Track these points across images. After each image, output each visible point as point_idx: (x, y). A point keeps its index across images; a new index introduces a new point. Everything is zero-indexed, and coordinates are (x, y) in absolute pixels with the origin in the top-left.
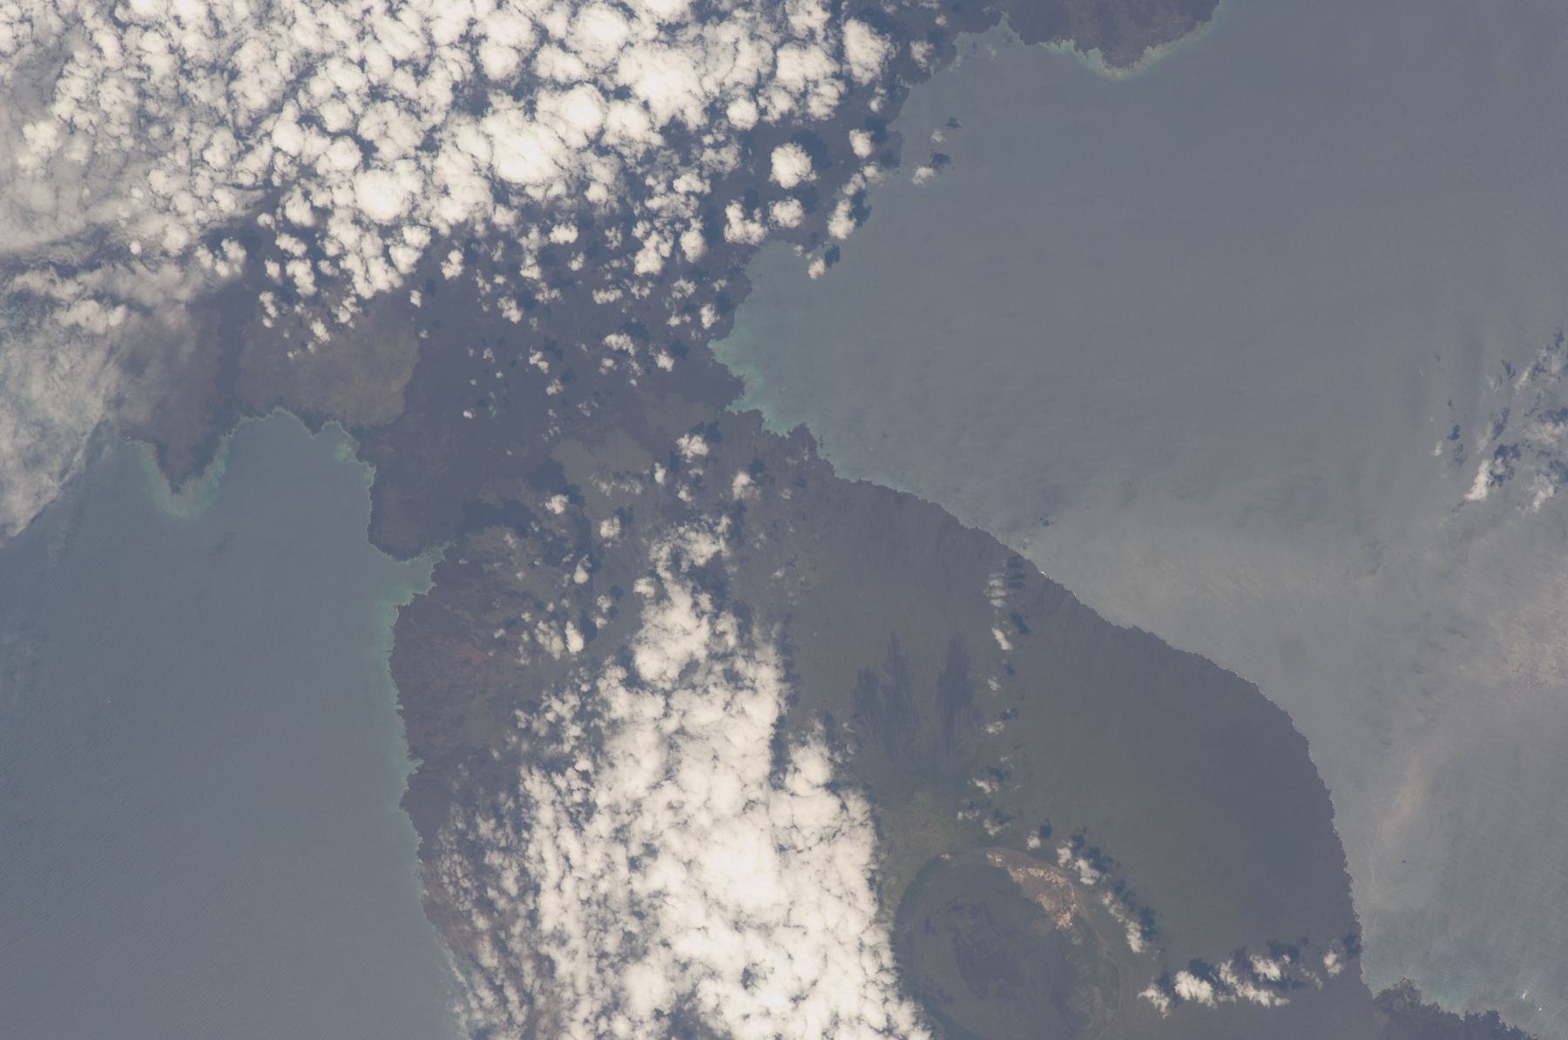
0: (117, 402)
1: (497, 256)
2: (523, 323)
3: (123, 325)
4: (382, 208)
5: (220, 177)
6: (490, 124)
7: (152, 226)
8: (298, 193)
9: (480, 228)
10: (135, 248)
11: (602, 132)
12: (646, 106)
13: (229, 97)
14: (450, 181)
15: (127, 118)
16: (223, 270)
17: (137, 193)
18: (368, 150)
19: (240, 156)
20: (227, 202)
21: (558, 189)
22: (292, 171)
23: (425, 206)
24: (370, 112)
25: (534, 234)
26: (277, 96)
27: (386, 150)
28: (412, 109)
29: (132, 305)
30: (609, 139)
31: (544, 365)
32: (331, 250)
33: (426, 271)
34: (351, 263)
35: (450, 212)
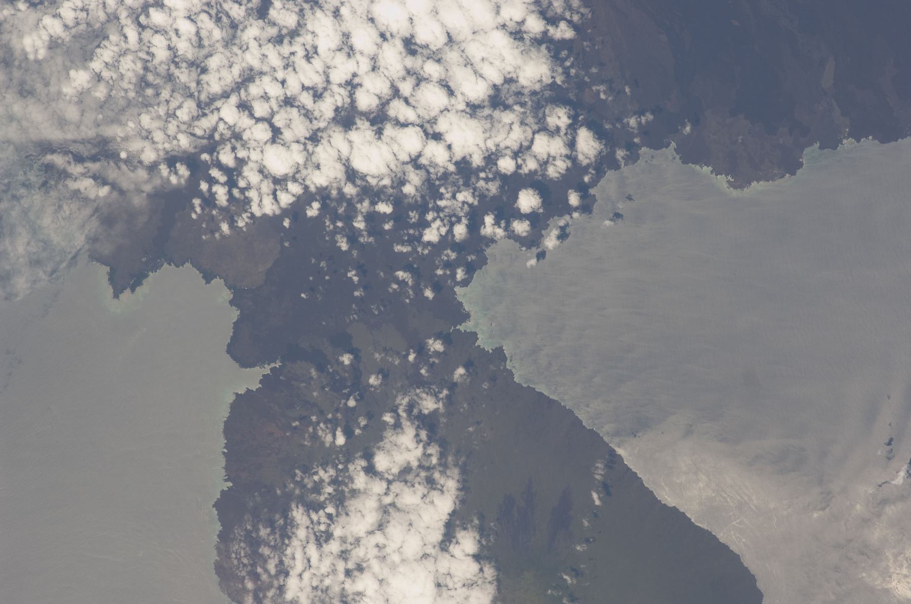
0: (93, 240)
1: (341, 210)
2: (349, 252)
3: (105, 197)
4: (276, 168)
5: (184, 127)
6: (353, 135)
7: (136, 145)
8: (228, 147)
9: (334, 193)
10: (123, 155)
11: (420, 155)
12: (449, 147)
13: (198, 83)
14: (322, 162)
15: (134, 80)
16: (174, 180)
17: (131, 124)
18: (276, 132)
19: (197, 118)
20: (184, 142)
21: (386, 182)
22: (228, 134)
23: (304, 172)
24: (282, 111)
25: (366, 204)
26: (228, 89)
27: (287, 135)
28: (308, 115)
29: (114, 186)
30: (423, 161)
31: (356, 279)
32: (242, 184)
33: (296, 210)
34: (252, 194)
35: (318, 179)
